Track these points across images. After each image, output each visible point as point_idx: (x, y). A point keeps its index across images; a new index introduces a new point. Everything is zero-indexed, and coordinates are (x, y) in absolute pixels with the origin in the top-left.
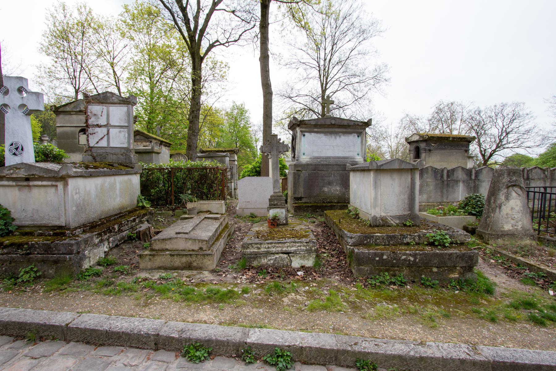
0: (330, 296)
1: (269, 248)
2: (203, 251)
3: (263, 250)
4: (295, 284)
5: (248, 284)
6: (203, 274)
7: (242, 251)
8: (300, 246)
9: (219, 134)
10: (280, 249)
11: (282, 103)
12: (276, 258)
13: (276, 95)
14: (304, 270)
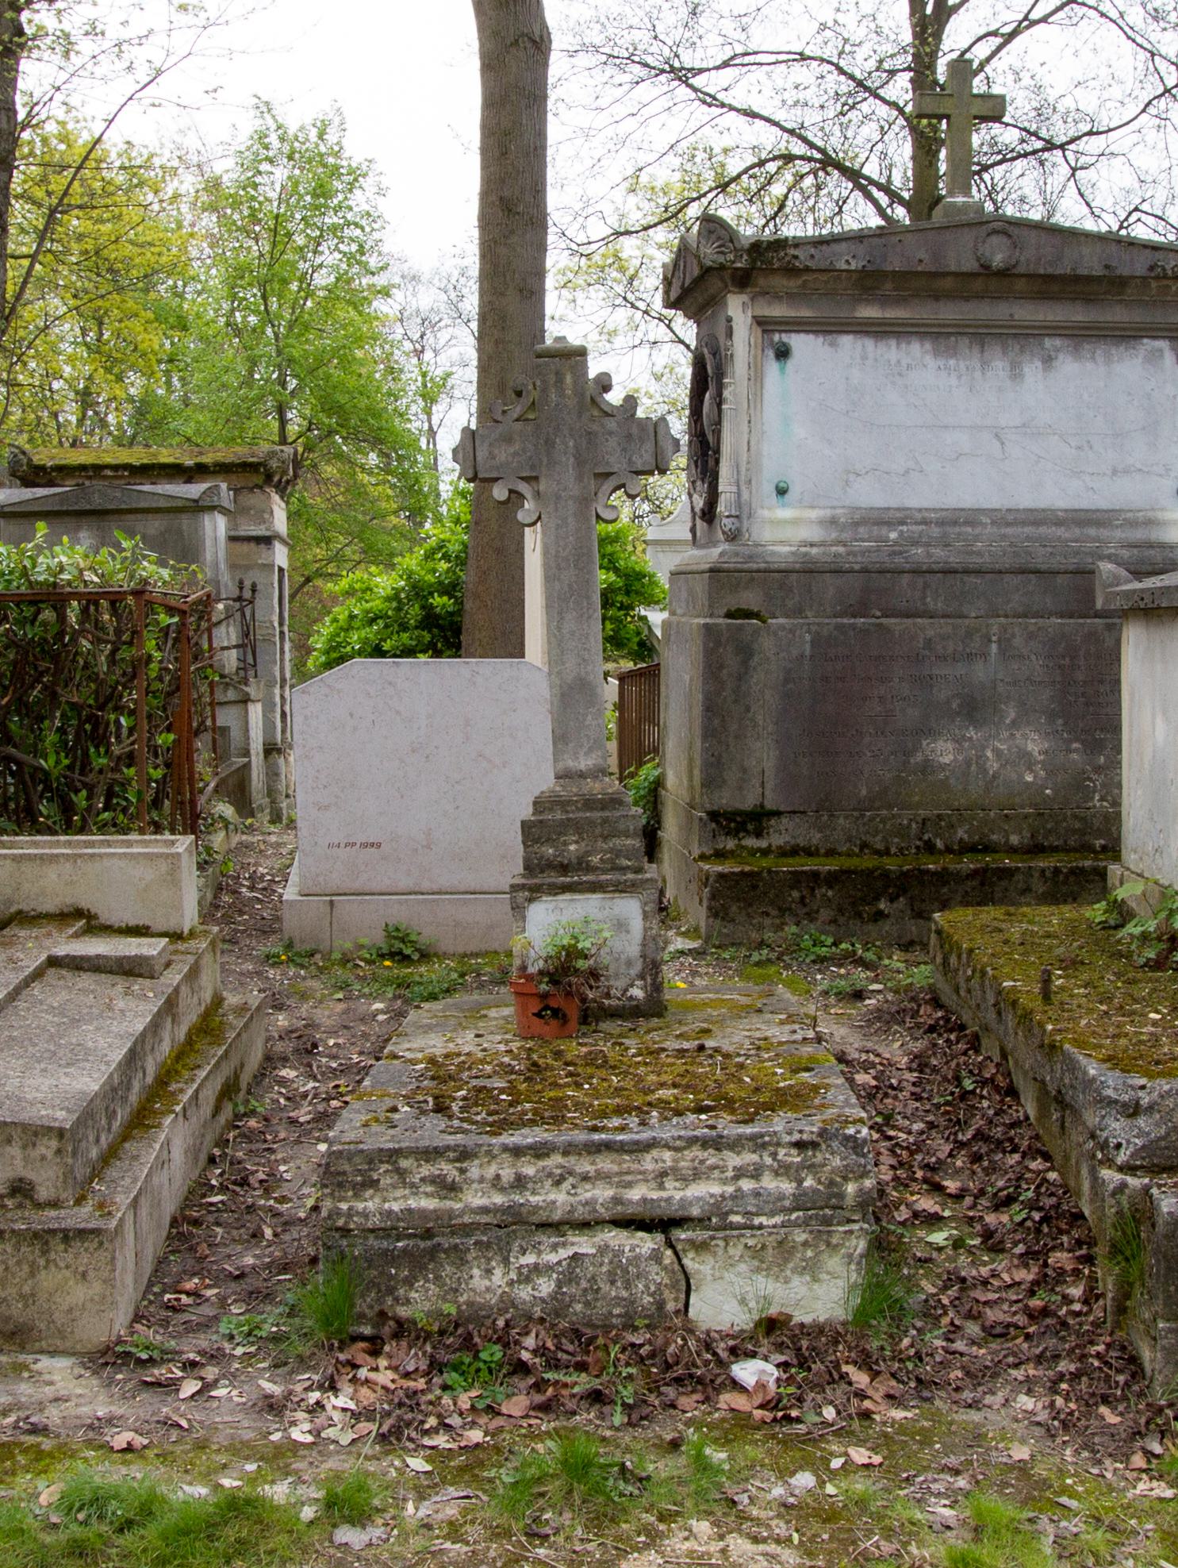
0: (977, 1540)
1: (520, 1182)
2: (39, 1206)
3: (478, 1201)
4: (718, 1456)
5: (367, 1449)
6: (34, 1377)
7: (327, 1205)
8: (756, 1173)
9: (157, 341)
10: (602, 1193)
11: (620, 110)
12: (575, 1257)
13: (572, 54)
14: (780, 1347)
